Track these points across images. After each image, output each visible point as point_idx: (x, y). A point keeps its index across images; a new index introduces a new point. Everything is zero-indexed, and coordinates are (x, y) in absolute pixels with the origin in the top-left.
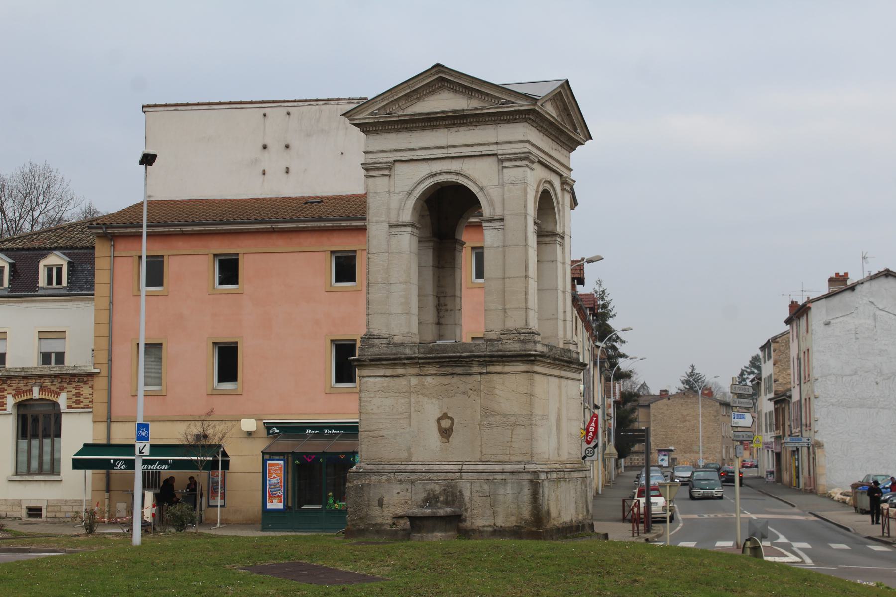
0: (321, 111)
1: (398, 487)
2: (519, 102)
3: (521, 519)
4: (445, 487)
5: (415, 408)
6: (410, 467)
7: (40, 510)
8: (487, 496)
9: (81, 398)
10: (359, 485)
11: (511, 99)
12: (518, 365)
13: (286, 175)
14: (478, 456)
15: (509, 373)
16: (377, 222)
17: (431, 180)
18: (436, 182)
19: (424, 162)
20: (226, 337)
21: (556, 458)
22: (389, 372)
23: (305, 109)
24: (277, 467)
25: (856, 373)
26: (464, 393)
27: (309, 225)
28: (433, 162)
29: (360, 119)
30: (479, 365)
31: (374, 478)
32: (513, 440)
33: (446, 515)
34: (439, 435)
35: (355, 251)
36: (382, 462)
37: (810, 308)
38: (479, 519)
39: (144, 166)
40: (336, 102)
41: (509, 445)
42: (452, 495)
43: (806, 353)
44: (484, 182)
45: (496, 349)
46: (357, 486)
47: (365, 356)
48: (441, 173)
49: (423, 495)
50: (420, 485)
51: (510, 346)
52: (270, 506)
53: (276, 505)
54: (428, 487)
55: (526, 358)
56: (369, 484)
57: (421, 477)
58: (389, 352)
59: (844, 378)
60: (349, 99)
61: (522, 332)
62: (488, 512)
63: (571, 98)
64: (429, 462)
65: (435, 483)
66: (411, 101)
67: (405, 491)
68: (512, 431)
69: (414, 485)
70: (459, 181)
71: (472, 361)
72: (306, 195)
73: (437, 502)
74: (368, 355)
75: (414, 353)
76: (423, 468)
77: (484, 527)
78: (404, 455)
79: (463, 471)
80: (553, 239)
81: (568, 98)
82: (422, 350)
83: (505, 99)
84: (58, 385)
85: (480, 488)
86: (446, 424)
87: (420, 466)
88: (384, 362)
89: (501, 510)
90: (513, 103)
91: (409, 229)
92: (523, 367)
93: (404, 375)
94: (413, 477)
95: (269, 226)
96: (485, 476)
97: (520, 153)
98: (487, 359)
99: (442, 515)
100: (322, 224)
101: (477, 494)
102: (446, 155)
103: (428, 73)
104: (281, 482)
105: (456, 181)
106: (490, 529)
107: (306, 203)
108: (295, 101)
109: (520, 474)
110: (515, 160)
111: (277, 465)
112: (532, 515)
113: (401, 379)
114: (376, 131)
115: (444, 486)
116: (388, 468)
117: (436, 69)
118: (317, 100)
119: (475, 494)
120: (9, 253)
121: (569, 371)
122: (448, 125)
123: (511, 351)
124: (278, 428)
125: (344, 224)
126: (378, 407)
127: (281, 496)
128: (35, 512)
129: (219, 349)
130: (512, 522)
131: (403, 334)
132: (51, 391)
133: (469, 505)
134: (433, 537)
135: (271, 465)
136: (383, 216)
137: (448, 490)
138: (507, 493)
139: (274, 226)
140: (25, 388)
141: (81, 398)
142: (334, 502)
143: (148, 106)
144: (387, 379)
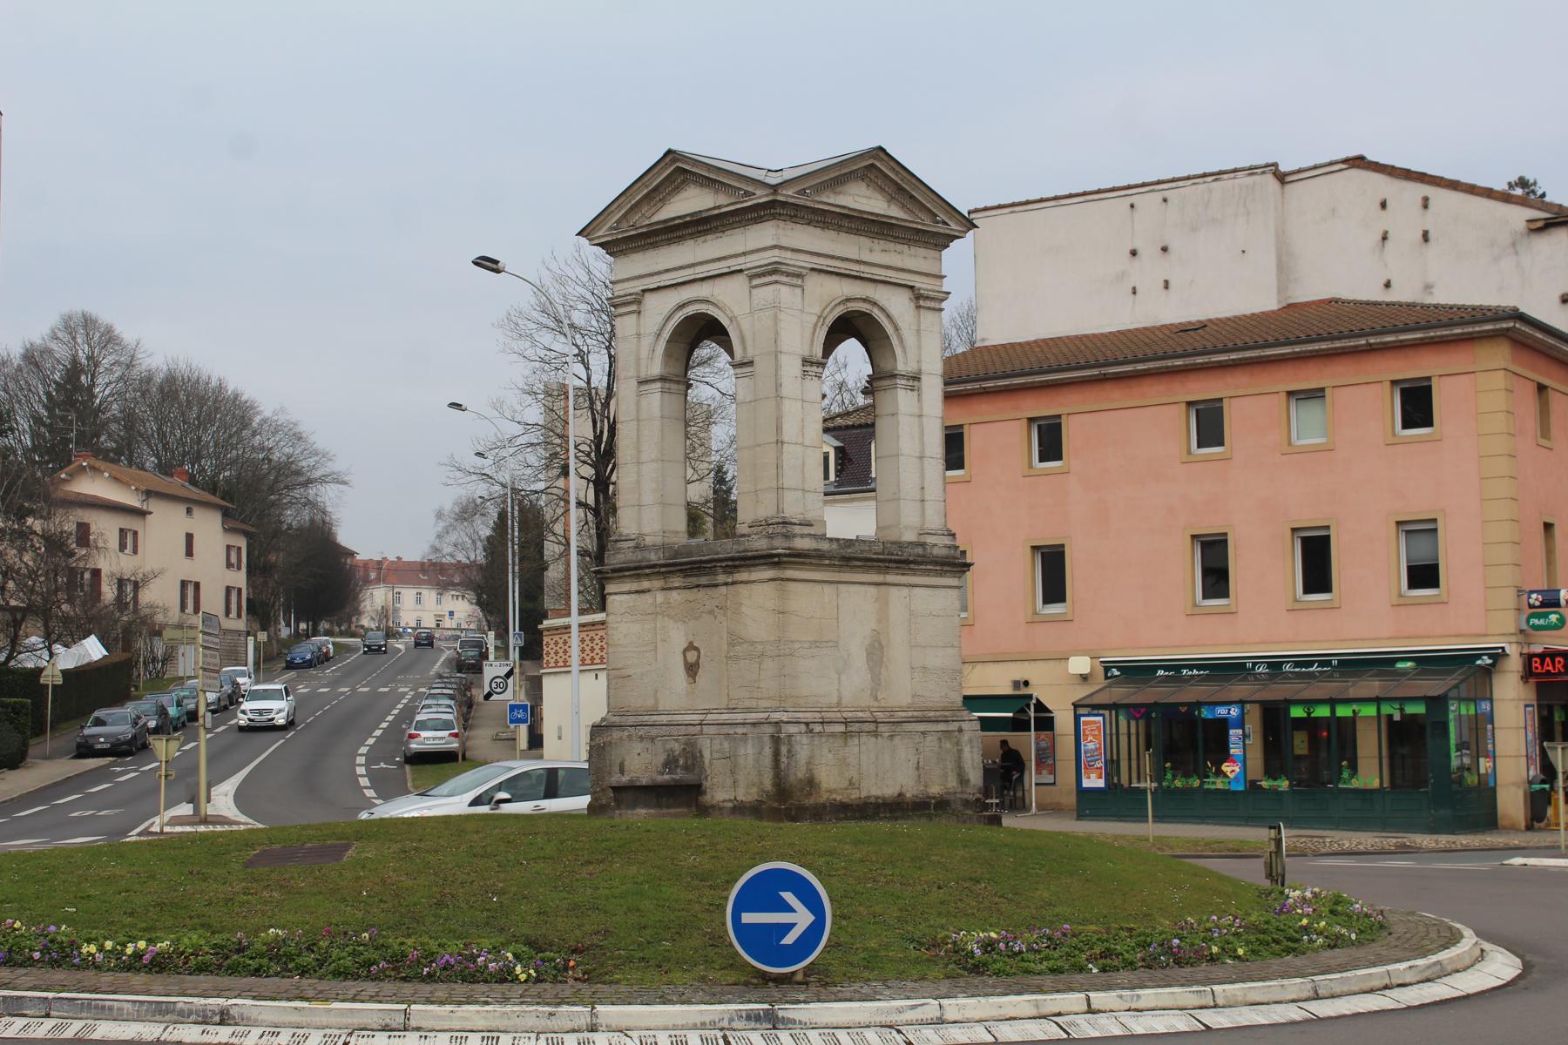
0: (1210, 191)
1: (638, 747)
2: (758, 193)
3: (763, 791)
6: (664, 719)
11: (750, 189)
12: (765, 570)
13: (1165, 292)
14: (724, 703)
15: (755, 581)
17: (680, 313)
19: (673, 289)
21: (866, 701)
22: (634, 586)
23: (1188, 190)
24: (1093, 727)
27: (1151, 365)
28: (684, 287)
29: (599, 237)
30: (724, 573)
31: (616, 734)
33: (651, 784)
35: (1221, 400)
38: (719, 792)
40: (1232, 175)
41: (756, 685)
42: (693, 758)
45: (741, 548)
48: (690, 303)
49: (662, 758)
50: (660, 743)
51: (757, 544)
52: (1086, 784)
53: (1094, 781)
54: (668, 747)
55: (770, 560)
56: (610, 743)
57: (662, 733)
58: (634, 558)
63: (902, 172)
66: (655, 205)
68: (760, 664)
71: (715, 566)
73: (677, 767)
75: (659, 559)
77: (724, 801)
78: (650, 703)
80: (893, 381)
81: (897, 173)
82: (667, 554)
86: (692, 657)
88: (627, 573)
89: (741, 777)
91: (658, 385)
92: (770, 573)
94: (654, 731)
95: (1095, 372)
96: (726, 730)
97: (766, 265)
98: (730, 563)
99: (644, 784)
100: (1169, 363)
102: (693, 277)
103: (663, 164)
104: (1100, 748)
106: (730, 805)
108: (1173, 180)
111: (1094, 722)
113: (647, 596)
114: (621, 251)
116: (631, 720)
117: (670, 157)
118: (1205, 175)
120: (837, 433)
121: (908, 574)
122: (693, 234)
124: (1118, 668)
125: (1200, 360)
126: (625, 636)
127: (1101, 768)
133: (709, 772)
134: (633, 815)
135: (1086, 723)
138: (748, 752)
139: (1104, 370)
143: (977, 211)
144: (633, 596)
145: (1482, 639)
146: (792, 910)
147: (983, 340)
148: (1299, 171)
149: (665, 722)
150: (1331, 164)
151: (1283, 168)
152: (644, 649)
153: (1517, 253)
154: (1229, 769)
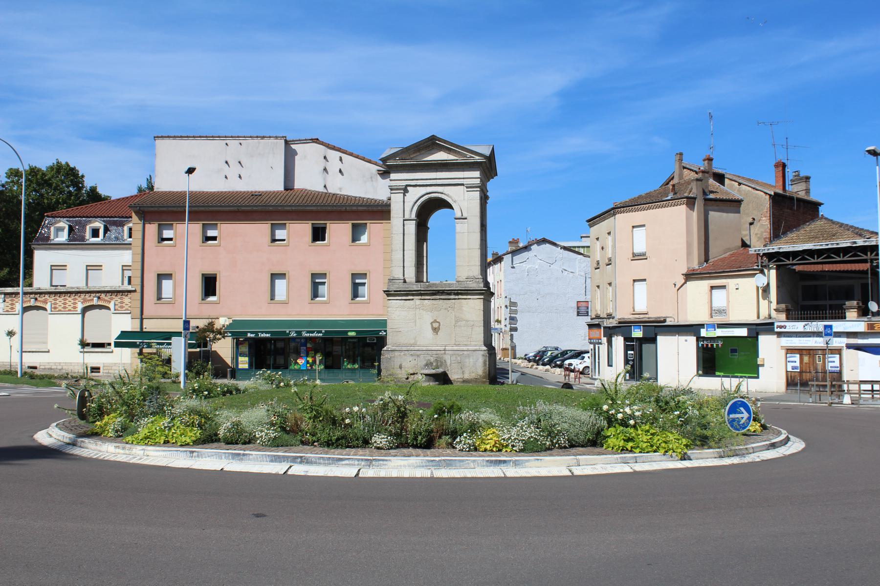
0: (259, 143)
2: (477, 158)
3: (478, 375)
6: (416, 348)
7: (99, 368)
9: (124, 305)
20: (209, 271)
26: (446, 309)
31: (397, 353)
37: (503, 258)
39: (187, 174)
41: (470, 336)
42: (439, 362)
43: (499, 282)
44: (456, 198)
46: (387, 358)
49: (425, 362)
54: (427, 358)
56: (394, 357)
58: (404, 287)
60: (276, 137)
62: (460, 371)
68: (472, 328)
72: (253, 190)
76: (424, 348)
77: (457, 379)
78: (412, 342)
84: (109, 297)
86: (436, 325)
93: (413, 299)
94: (419, 353)
101: (454, 362)
106: (462, 380)
107: (252, 195)
110: (473, 187)
112: (484, 373)
128: (96, 369)
129: (205, 277)
130: (473, 376)
132: (105, 301)
133: (449, 368)
140: (90, 298)
141: (124, 305)
142: (348, 364)
143: (158, 137)
145: (383, 316)
146: (743, 413)
147: (158, 188)
148: (293, 141)
150: (306, 140)
151: (288, 139)
153: (372, 181)
154: (300, 362)
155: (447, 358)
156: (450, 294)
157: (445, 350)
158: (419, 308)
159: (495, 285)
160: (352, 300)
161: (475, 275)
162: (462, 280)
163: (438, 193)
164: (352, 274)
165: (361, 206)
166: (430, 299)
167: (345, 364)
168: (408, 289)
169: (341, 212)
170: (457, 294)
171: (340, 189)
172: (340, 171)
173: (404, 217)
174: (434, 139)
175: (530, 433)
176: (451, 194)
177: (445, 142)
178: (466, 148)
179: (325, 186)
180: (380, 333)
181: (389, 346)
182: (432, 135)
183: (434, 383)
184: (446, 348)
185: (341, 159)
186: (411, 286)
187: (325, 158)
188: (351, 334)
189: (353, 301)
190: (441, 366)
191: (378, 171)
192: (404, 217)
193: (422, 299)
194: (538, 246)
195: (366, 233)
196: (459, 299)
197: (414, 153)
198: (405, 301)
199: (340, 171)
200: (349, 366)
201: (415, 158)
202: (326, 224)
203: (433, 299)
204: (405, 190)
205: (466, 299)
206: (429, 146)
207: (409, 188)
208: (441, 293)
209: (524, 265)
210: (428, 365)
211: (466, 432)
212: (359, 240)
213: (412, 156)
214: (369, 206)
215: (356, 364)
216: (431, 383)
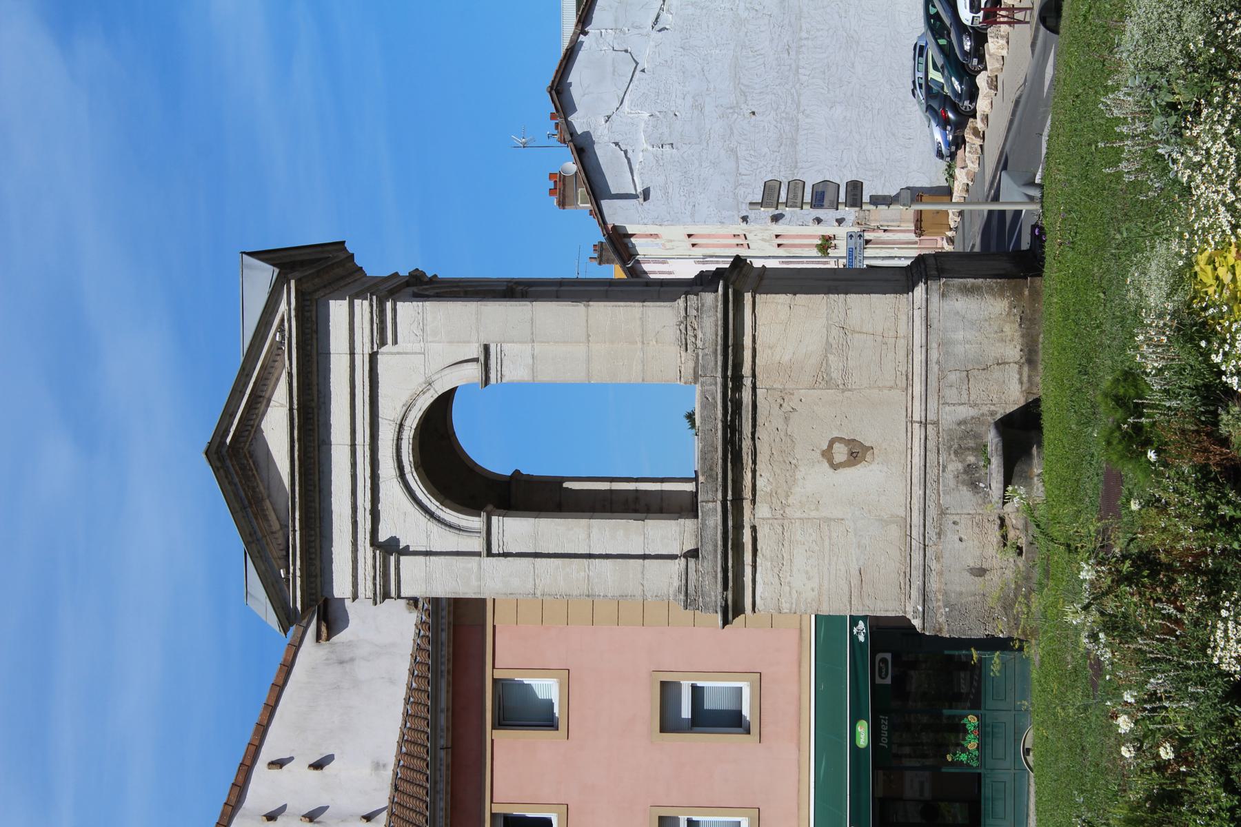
1: (951, 537)
2: (283, 307)
4: (952, 452)
5: (812, 511)
8: (967, 376)
10: (946, 612)
14: (898, 395)
16: (479, 579)
18: (413, 469)
25: (733, 151)
26: (786, 419)
31: (934, 584)
32: (871, 331)
34: (859, 465)
36: (905, 573)
37: (614, 227)
41: (879, 339)
43: (694, 240)
44: (417, 382)
46: (948, 616)
47: (716, 602)
49: (965, 492)
54: (952, 483)
56: (946, 594)
58: (710, 557)
59: (742, 170)
61: (683, 313)
62: (997, 373)
64: (906, 486)
65: (943, 471)
67: (957, 527)
69: (947, 509)
70: (414, 426)
74: (716, 596)
76: (918, 492)
77: (1021, 383)
78: (895, 532)
79: (924, 421)
83: (275, 335)
85: (954, 390)
86: (841, 453)
87: (915, 500)
90: (282, 320)
93: (754, 529)
94: (932, 512)
97: (372, 313)
101: (964, 393)
105: (413, 431)
106: (1026, 369)
109: (931, 315)
112: (1002, 295)
115: (950, 454)
116: (917, 558)
119: (965, 397)
123: (717, 331)
130: (1012, 330)
131: (680, 533)
133: (985, 409)
136: (470, 565)
137: (956, 446)
145: (806, 635)
149: (921, 492)
152: (827, 543)
153: (352, 660)
155: (953, 414)
156: (738, 405)
157: (924, 424)
158: (783, 506)
159: (705, 257)
160: (748, 732)
161: (675, 321)
162: (691, 364)
163: (399, 439)
164: (663, 730)
165: (434, 697)
166: (754, 472)
167: (964, 757)
168: (720, 543)
169: (456, 768)
170: (738, 379)
171: (378, 766)
172: (318, 766)
173: (478, 554)
174: (218, 452)
175: (1215, 138)
176: (405, 397)
177: (228, 414)
178: (251, 345)
179: (368, 818)
180: (862, 638)
181: (909, 609)
182: (204, 456)
183: (1035, 461)
184: (916, 418)
185: (278, 764)
186: (709, 533)
187: (271, 817)
188: (863, 739)
189: (754, 729)
190: (977, 436)
191: (318, 637)
192: (478, 554)
193: (754, 495)
194: (574, 110)
195: (526, 681)
196: (754, 376)
197: (266, 518)
198: (759, 554)
199: (318, 766)
200: (972, 744)
201: (283, 515)
202: (493, 815)
203: (754, 462)
204: (390, 549)
205: (754, 350)
206: (243, 468)
207: (383, 537)
208: (733, 434)
209: (637, 159)
210: (972, 479)
211: (1206, 355)
212: (550, 704)
213: (276, 526)
214: (435, 670)
215: (965, 721)
216: (1037, 471)
